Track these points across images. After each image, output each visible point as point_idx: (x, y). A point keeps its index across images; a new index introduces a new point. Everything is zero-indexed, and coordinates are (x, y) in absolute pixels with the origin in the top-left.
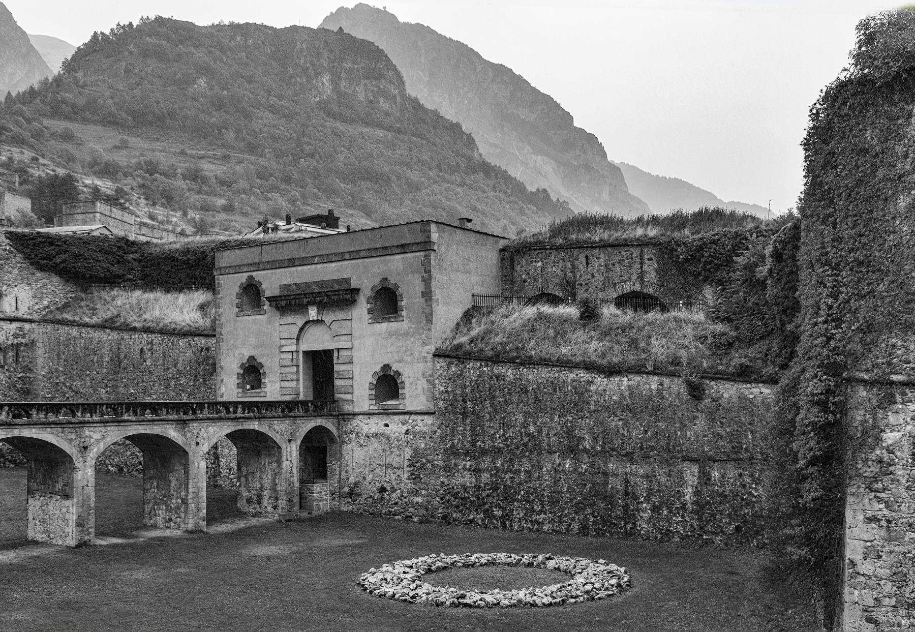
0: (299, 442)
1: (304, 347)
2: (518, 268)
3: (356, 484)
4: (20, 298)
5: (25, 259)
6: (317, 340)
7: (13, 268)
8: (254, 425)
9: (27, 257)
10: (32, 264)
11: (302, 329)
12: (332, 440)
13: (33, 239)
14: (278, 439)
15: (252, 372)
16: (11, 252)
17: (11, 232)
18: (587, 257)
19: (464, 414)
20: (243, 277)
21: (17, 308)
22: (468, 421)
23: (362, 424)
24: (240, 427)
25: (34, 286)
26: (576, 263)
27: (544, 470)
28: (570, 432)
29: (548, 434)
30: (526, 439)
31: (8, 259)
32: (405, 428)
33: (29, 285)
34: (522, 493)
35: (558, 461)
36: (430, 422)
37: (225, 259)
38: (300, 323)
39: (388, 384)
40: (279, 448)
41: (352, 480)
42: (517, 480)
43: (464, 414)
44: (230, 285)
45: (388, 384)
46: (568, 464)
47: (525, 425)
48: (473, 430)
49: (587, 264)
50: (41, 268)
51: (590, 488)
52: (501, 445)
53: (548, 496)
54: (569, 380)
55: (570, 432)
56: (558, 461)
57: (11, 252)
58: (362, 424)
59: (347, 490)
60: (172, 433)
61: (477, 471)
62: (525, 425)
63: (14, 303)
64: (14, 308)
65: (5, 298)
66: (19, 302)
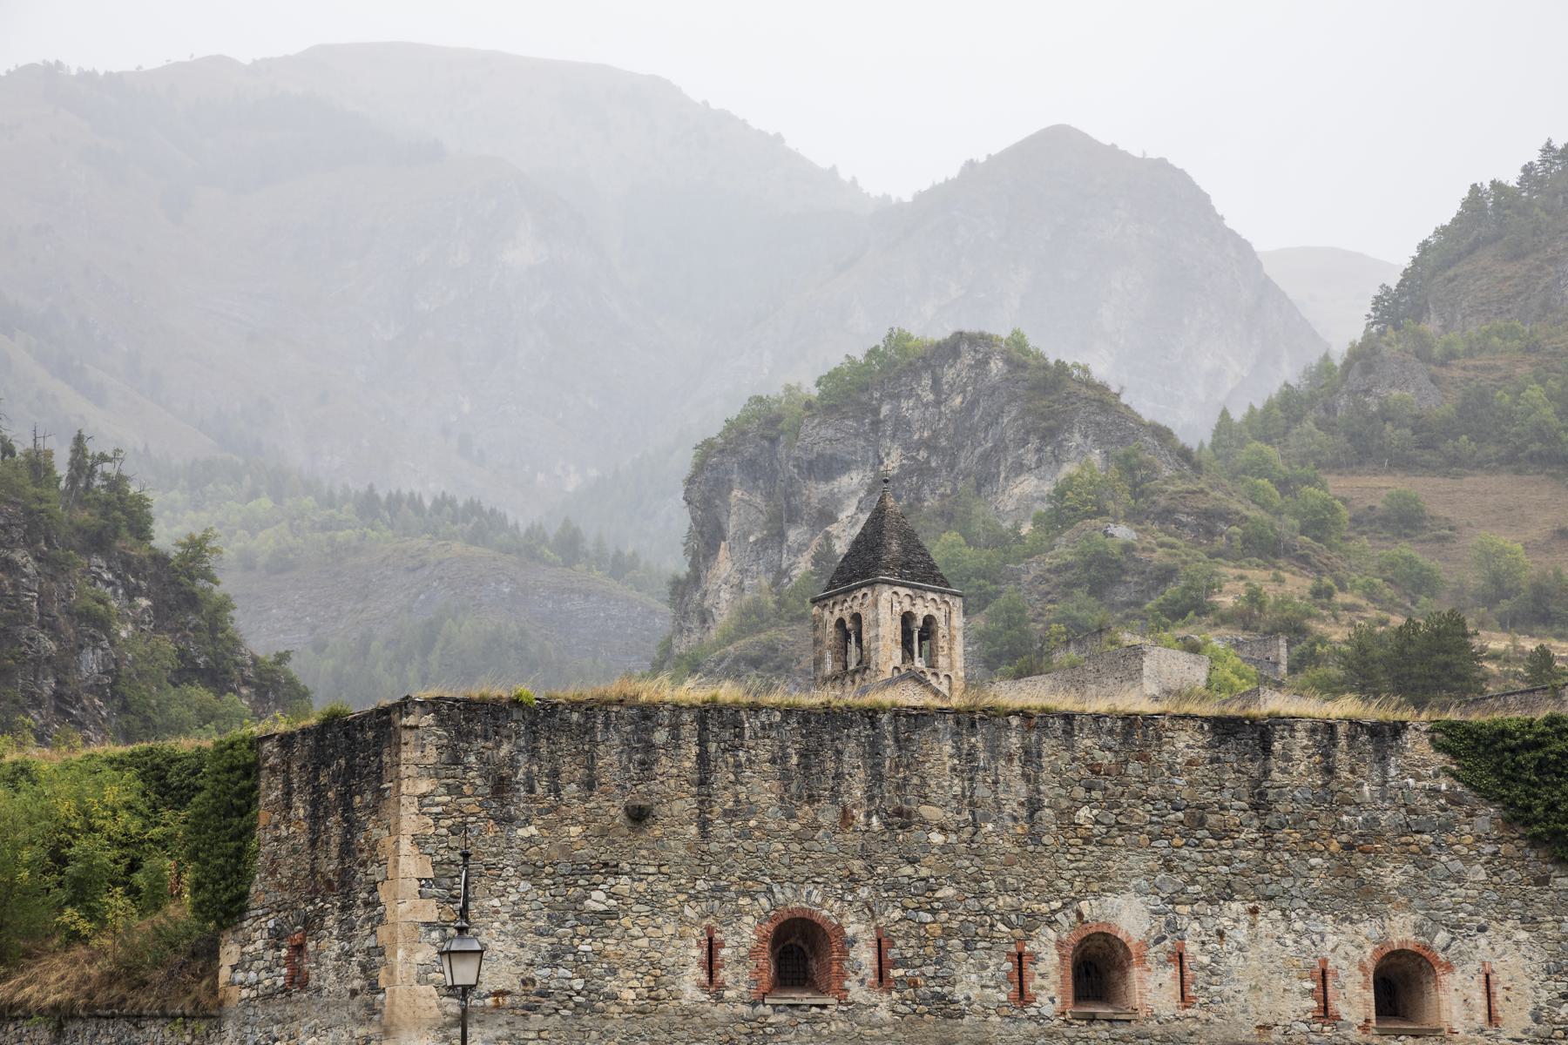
4: (1501, 978)
5: (1509, 823)
7: (1466, 859)
9: (1517, 817)
10: (1535, 841)
13: (1537, 745)
16: (1455, 800)
17: (1453, 725)
21: (1491, 1017)
25: (1548, 927)
31: (1446, 828)
33: (1531, 923)
57: (1455, 800)
63: (1479, 999)
64: (1481, 1017)
65: (1446, 979)
66: (1500, 994)
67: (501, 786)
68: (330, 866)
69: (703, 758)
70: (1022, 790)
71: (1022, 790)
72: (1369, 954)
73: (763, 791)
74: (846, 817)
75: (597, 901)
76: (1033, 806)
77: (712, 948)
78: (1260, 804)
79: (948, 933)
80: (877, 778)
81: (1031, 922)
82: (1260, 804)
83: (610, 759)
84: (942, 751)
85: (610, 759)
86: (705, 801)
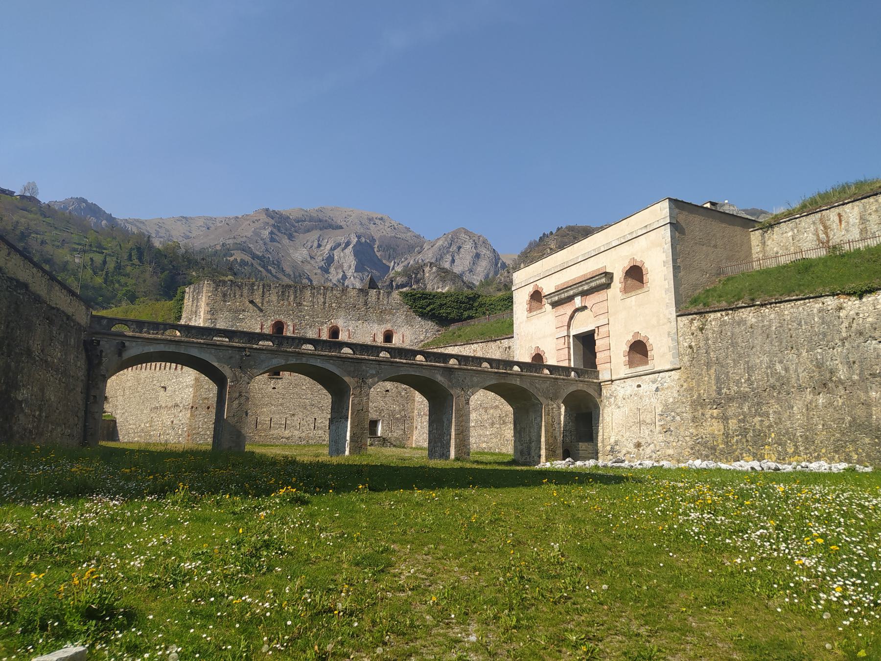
1: (573, 332)
2: (769, 242)
3: (616, 443)
18: (840, 215)
19: (708, 365)
22: (713, 371)
23: (619, 388)
24: (503, 381)
26: (828, 223)
27: (795, 408)
28: (819, 365)
29: (796, 371)
30: (772, 380)
32: (655, 386)
34: (773, 435)
35: (809, 397)
36: (677, 377)
38: (569, 313)
39: (639, 349)
41: (612, 440)
42: (766, 423)
43: (708, 365)
45: (639, 349)
46: (821, 400)
47: (771, 366)
48: (718, 379)
49: (840, 221)
50: (423, 316)
51: (850, 422)
52: (747, 389)
53: (801, 436)
54: (815, 311)
55: (819, 365)
56: (809, 397)
58: (619, 388)
59: (609, 448)
61: (725, 419)
62: (771, 366)
67: (224, 295)
68: (194, 309)
69: (263, 292)
70: (322, 300)
71: (322, 300)
72: (383, 330)
73: (274, 298)
74: (290, 304)
75: (241, 316)
76: (325, 303)
77: (262, 326)
78: (366, 304)
79: (306, 325)
80: (296, 297)
81: (322, 323)
82: (366, 304)
83: (245, 291)
84: (308, 293)
85: (245, 291)
86: (263, 300)
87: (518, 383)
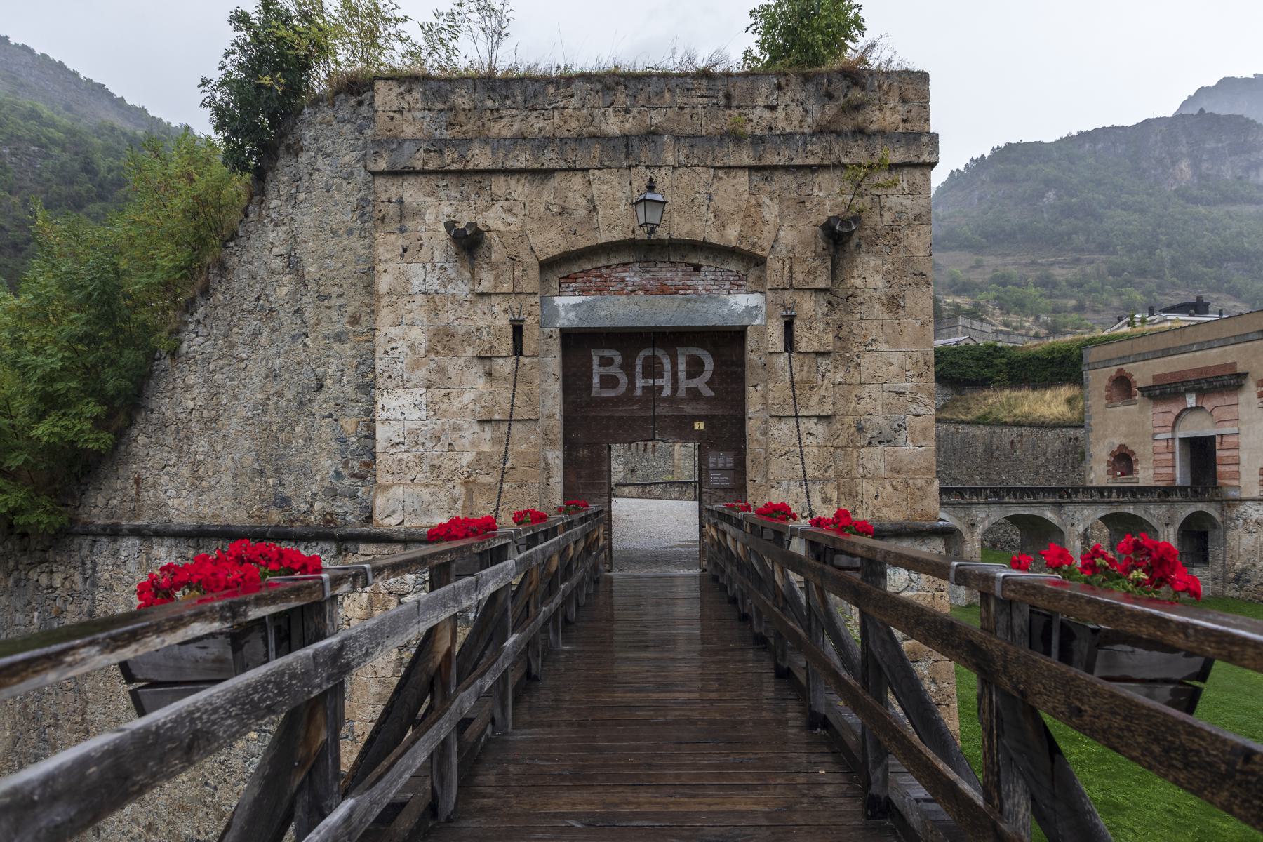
0: (1177, 526)
1: (1181, 434)
3: (1244, 571)
6: (1196, 427)
8: (1130, 509)
11: (1178, 417)
12: (1214, 525)
14: (1154, 522)
15: (1124, 460)
20: (1113, 371)
37: (1092, 355)
38: (1176, 411)
40: (1156, 531)
41: (1239, 565)
44: (1099, 379)
59: (1232, 575)
60: (1049, 515)
87: (1132, 511)
